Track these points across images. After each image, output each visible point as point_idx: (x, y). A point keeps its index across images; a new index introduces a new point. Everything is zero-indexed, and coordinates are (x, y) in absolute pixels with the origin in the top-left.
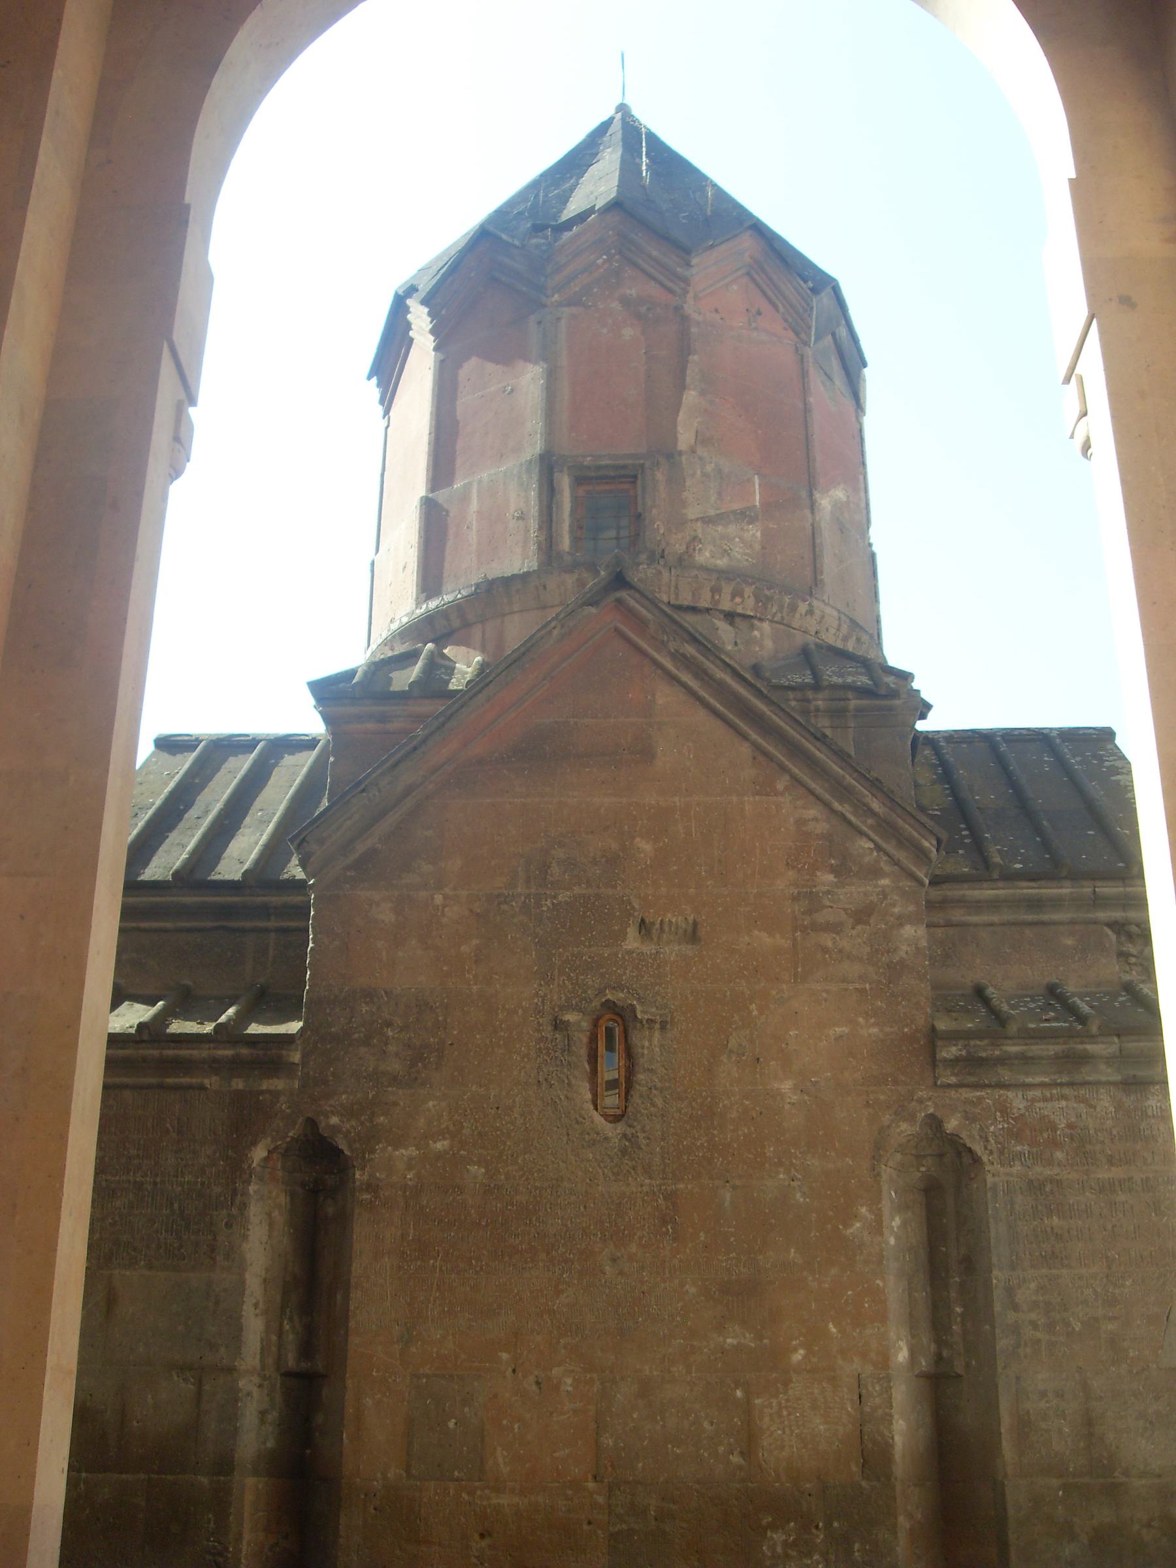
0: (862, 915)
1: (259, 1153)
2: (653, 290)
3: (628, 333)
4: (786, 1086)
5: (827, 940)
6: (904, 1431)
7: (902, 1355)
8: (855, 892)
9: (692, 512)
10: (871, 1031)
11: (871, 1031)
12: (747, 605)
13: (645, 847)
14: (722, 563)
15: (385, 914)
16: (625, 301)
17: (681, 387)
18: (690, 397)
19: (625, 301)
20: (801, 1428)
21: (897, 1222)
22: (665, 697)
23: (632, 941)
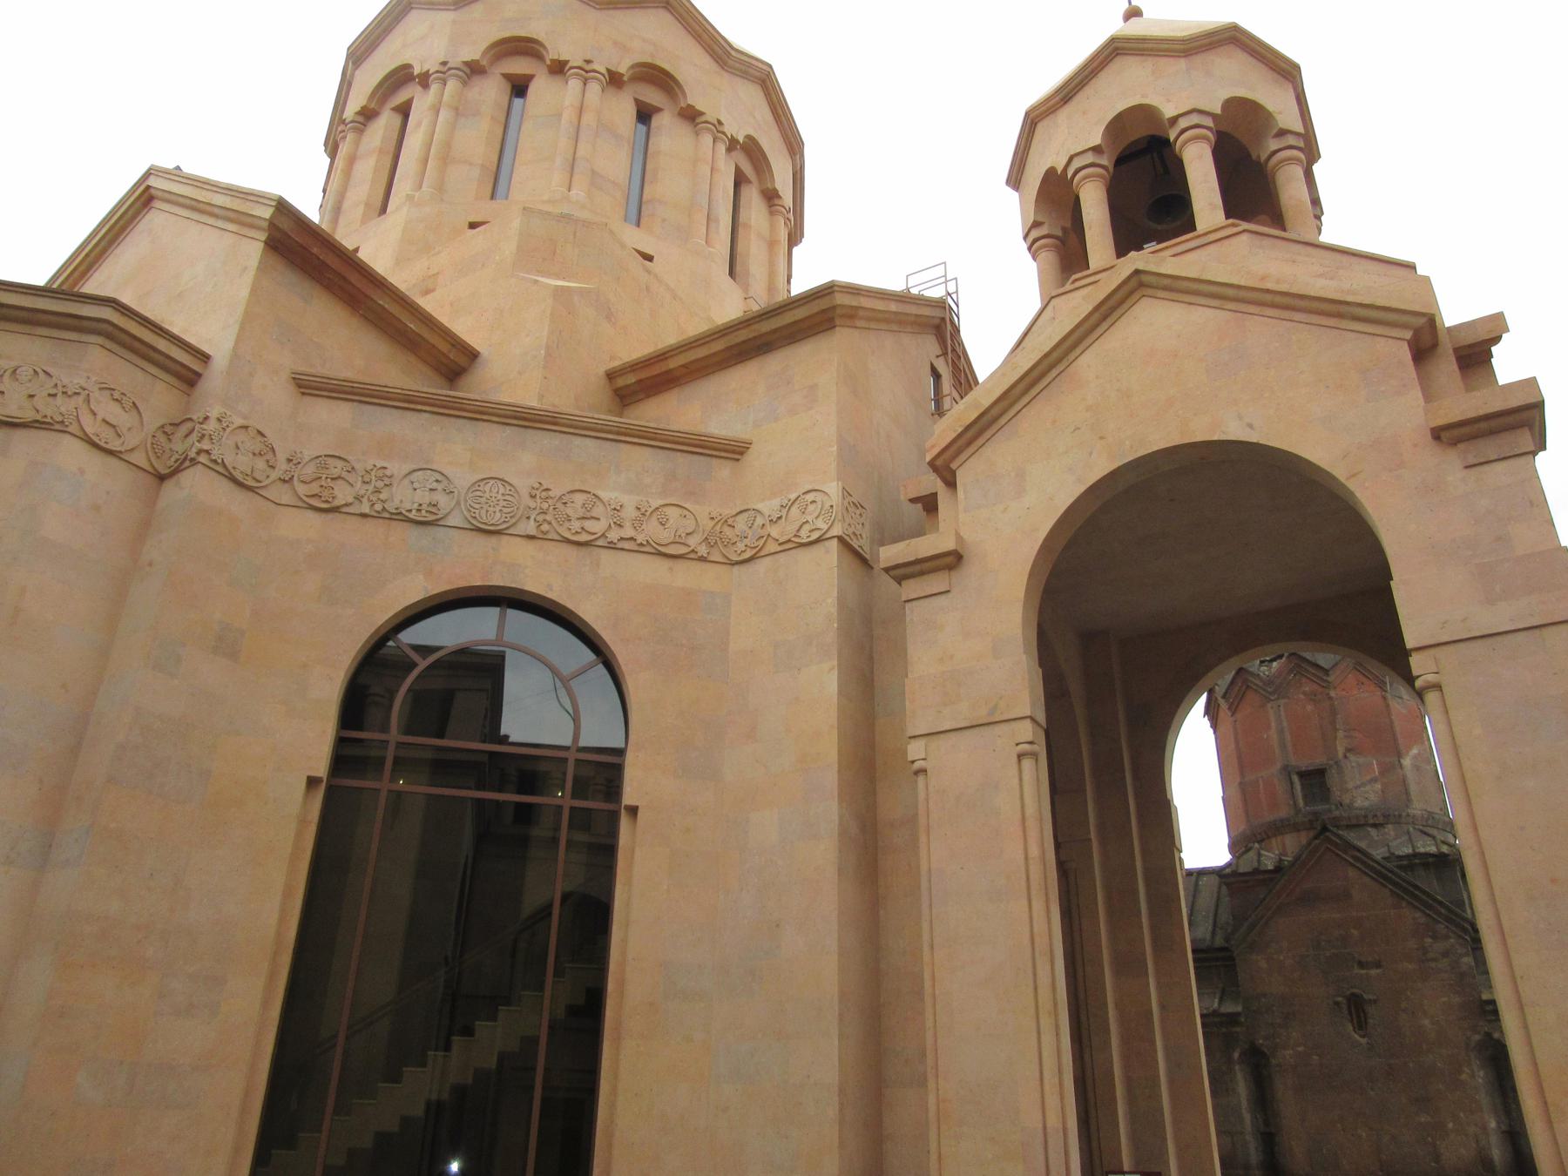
0: (1445, 954)
1: (1236, 1055)
2: (1315, 687)
3: (1309, 708)
4: (1426, 1022)
5: (1433, 965)
6: (1497, 1154)
7: (1493, 1125)
8: (1440, 946)
9: (1350, 785)
10: (1457, 1000)
11: (1457, 1000)
12: (1381, 820)
13: (1355, 932)
14: (1366, 804)
15: (1263, 964)
16: (1304, 693)
17: (1336, 730)
18: (1340, 734)
19: (1304, 693)
20: (1456, 1150)
21: (1482, 1073)
22: (1352, 873)
23: (1357, 971)
